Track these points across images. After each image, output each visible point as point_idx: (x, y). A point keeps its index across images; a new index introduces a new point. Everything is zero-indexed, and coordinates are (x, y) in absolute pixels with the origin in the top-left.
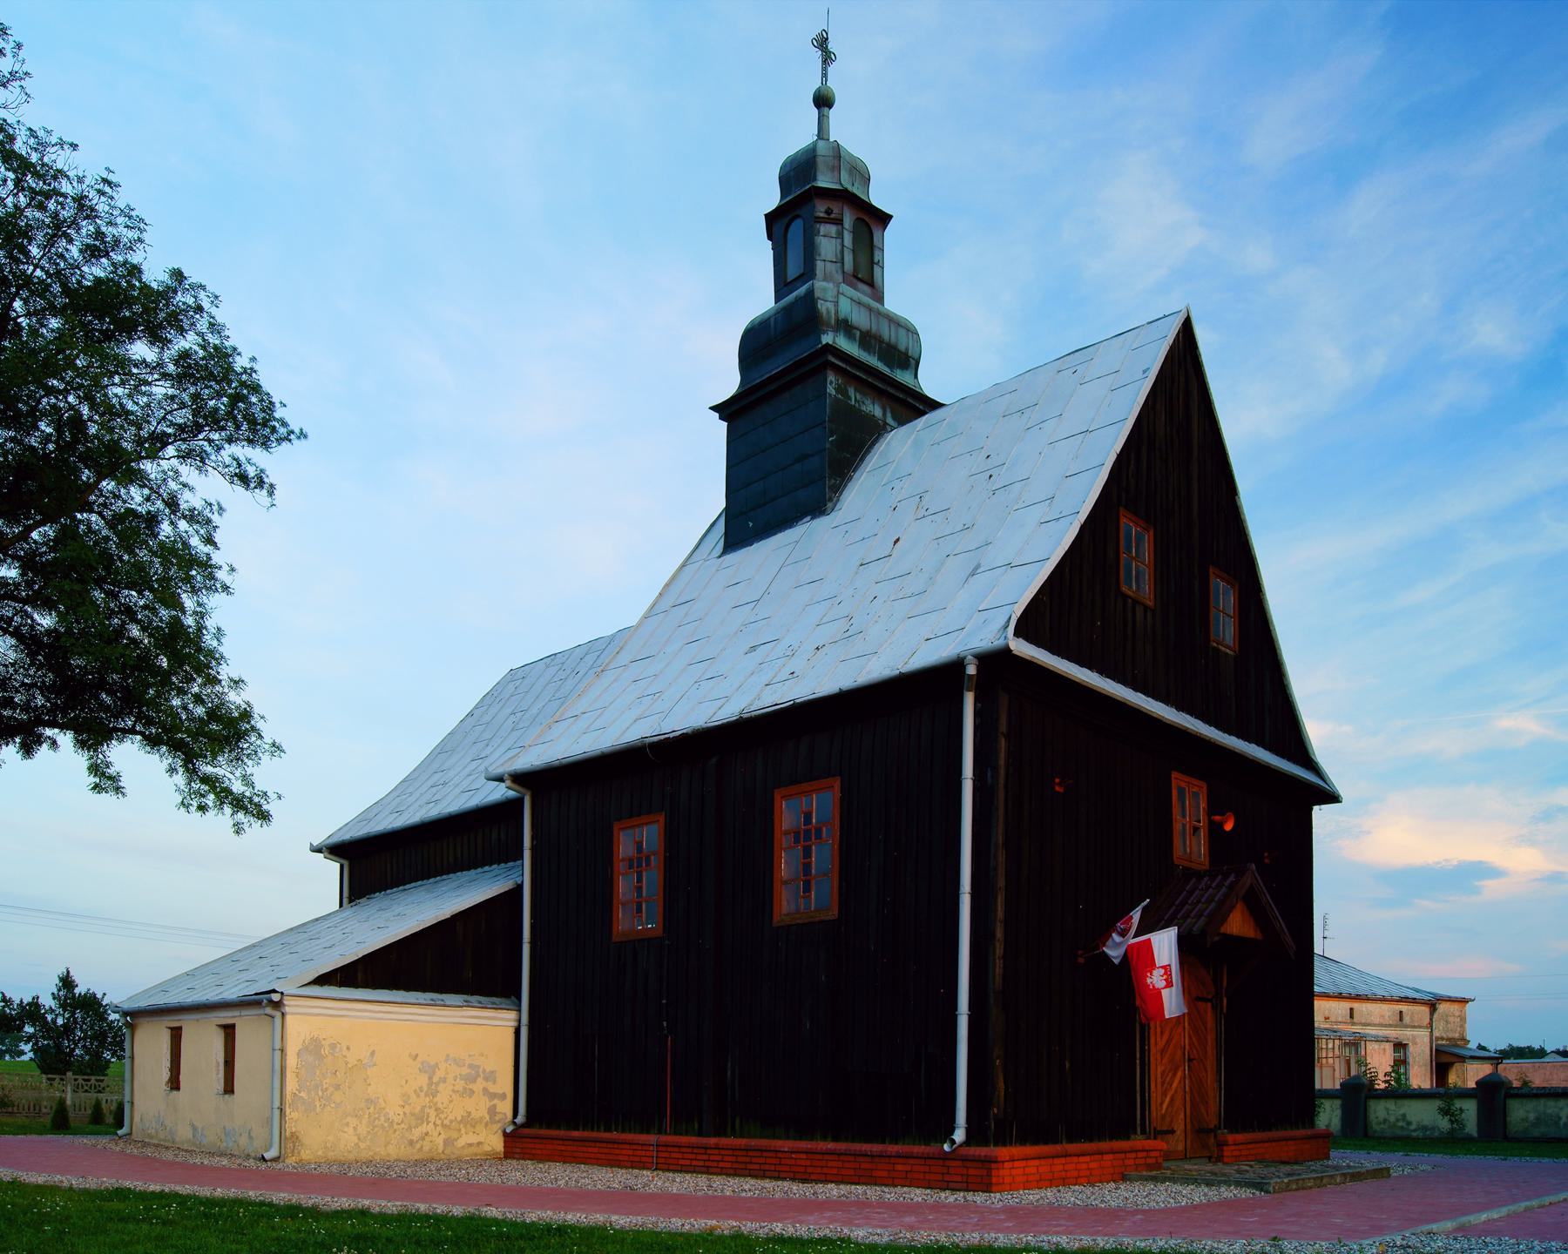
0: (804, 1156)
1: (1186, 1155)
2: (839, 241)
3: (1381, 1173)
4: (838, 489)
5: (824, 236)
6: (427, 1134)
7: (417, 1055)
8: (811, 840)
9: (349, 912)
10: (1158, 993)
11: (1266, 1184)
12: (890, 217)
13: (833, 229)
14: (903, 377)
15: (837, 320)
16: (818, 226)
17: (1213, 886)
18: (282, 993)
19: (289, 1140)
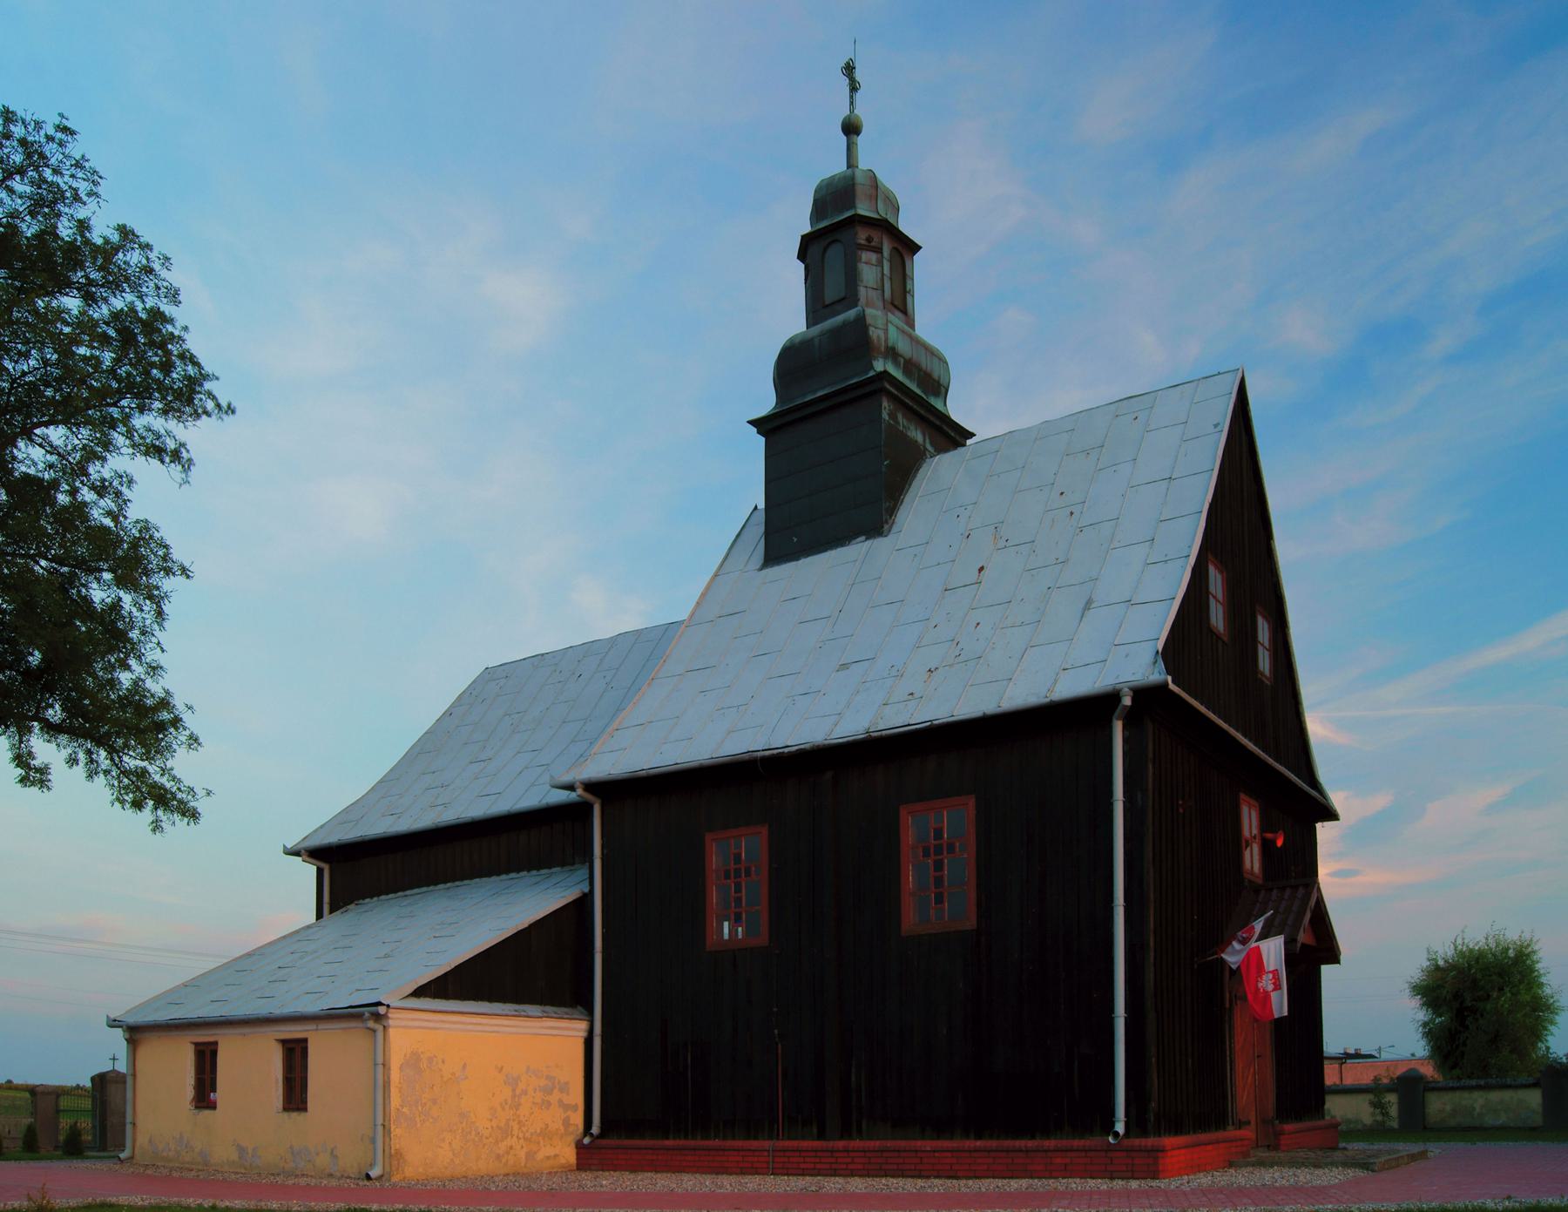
0: (949, 1155)
1: (1257, 1144)
2: (879, 269)
3: (1423, 1155)
4: (892, 511)
5: (866, 263)
6: (511, 1148)
7: (502, 1068)
8: (942, 854)
9: (340, 922)
10: (1267, 996)
11: (1372, 1163)
12: (918, 248)
13: (873, 257)
14: (936, 403)
15: (887, 347)
16: (860, 252)
17: (1286, 897)
18: (388, 1006)
19: (394, 1158)
